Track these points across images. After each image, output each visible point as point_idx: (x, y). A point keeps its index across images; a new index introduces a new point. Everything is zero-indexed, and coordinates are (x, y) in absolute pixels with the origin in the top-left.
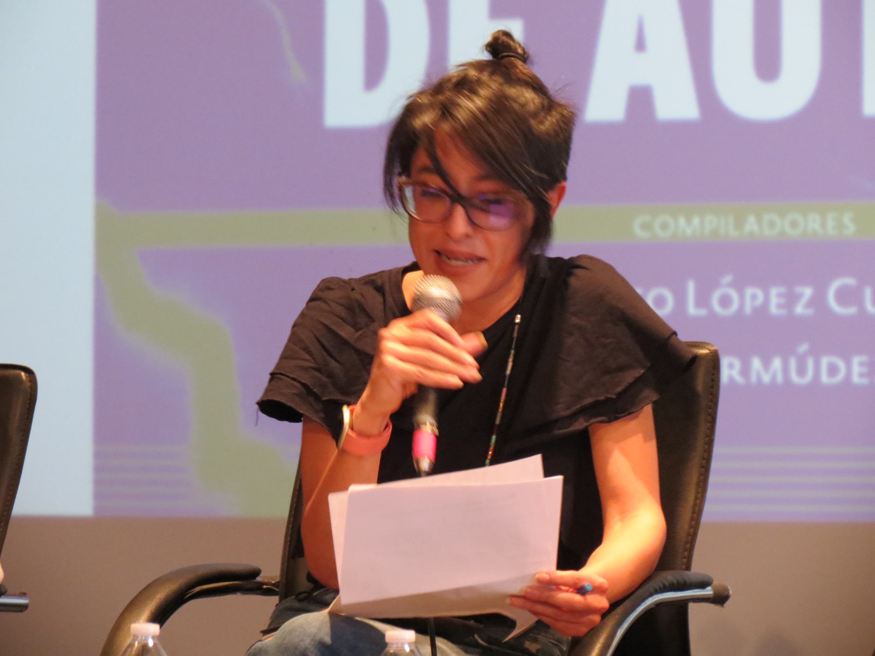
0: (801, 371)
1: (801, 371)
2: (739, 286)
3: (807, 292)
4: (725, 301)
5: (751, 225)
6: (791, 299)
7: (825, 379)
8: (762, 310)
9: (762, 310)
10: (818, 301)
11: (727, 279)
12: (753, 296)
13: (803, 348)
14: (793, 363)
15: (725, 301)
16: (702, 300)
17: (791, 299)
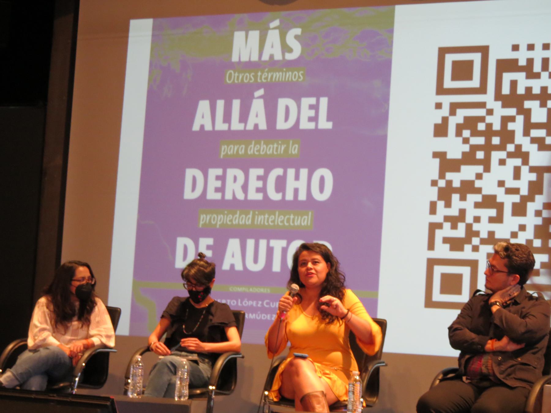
0: (258, 316)
1: (258, 316)
2: (248, 300)
3: (260, 302)
4: (246, 303)
5: (251, 290)
6: (257, 303)
7: (263, 318)
8: (252, 305)
9: (252, 305)
10: (262, 304)
11: (246, 299)
12: (250, 303)
13: (259, 312)
14: (257, 315)
15: (246, 303)
16: (241, 303)
17: (257, 303)
